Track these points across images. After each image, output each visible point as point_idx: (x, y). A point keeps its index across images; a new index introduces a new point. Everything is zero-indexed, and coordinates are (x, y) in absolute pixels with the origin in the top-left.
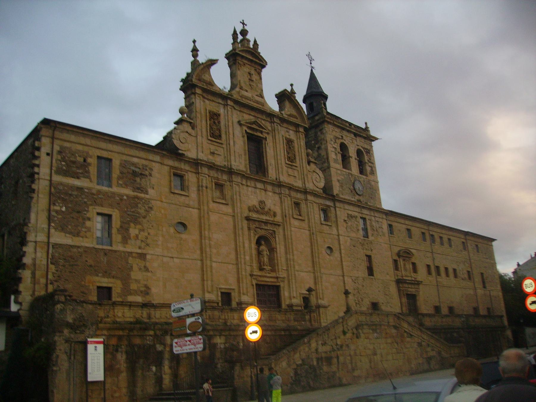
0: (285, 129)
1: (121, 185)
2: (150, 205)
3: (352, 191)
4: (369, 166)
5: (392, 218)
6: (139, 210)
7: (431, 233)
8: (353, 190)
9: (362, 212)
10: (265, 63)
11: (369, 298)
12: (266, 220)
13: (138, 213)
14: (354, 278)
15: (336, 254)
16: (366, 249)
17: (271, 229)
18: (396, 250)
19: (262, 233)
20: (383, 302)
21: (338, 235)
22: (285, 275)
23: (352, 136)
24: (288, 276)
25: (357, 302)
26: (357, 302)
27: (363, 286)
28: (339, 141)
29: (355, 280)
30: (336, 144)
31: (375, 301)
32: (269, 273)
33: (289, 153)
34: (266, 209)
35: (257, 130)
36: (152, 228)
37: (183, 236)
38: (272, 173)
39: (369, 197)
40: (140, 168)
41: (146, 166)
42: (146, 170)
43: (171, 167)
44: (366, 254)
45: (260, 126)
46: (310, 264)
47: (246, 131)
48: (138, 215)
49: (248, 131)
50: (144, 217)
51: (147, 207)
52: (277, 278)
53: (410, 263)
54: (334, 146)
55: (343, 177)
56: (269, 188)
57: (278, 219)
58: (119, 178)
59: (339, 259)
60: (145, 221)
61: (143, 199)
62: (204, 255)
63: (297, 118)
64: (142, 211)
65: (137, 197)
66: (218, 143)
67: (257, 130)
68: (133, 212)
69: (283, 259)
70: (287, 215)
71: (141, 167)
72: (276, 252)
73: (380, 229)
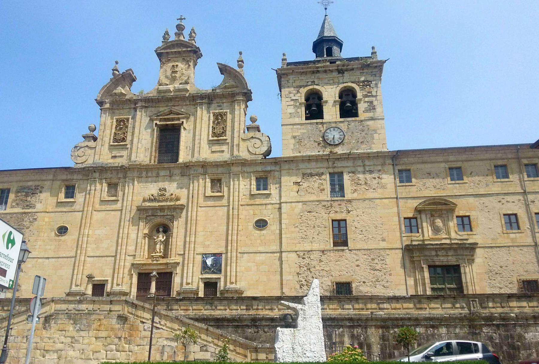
0: (217, 104)
1: (13, 206)
2: (35, 217)
3: (319, 144)
4: (365, 102)
5: (411, 159)
6: (24, 223)
7: (525, 161)
8: (321, 142)
9: (335, 165)
10: (194, 47)
11: (331, 277)
12: (159, 206)
13: (24, 225)
14: (301, 254)
15: (273, 227)
16: (336, 212)
17: (169, 214)
18: (415, 203)
19: (158, 220)
20: (364, 280)
21: (280, 204)
22: (179, 259)
23: (335, 74)
24: (184, 261)
25: (304, 282)
26: (304, 282)
27: (321, 261)
28: (303, 91)
29: (304, 254)
30: (299, 95)
31: (343, 280)
32: (157, 261)
33: (214, 128)
34: (167, 194)
35: (173, 119)
36: (33, 235)
37: (63, 238)
38: (183, 157)
39: (358, 142)
40: (32, 189)
41: (38, 186)
42: (38, 189)
43: (63, 180)
44: (334, 219)
45: (178, 114)
46: (223, 243)
47: (156, 124)
48: (22, 227)
49: (158, 123)
50: (28, 228)
51: (31, 220)
52: (167, 264)
53: (455, 217)
54: (294, 98)
55: (305, 131)
56: (177, 171)
57: (183, 201)
58: (14, 201)
59: (278, 231)
60: (27, 231)
61: (30, 213)
62: (79, 252)
63: (237, 87)
64: (27, 223)
65: (25, 213)
66: (121, 145)
67: (173, 119)
68: (19, 225)
69: (180, 243)
70: (195, 196)
71: (33, 188)
72: (172, 236)
73: (375, 181)
